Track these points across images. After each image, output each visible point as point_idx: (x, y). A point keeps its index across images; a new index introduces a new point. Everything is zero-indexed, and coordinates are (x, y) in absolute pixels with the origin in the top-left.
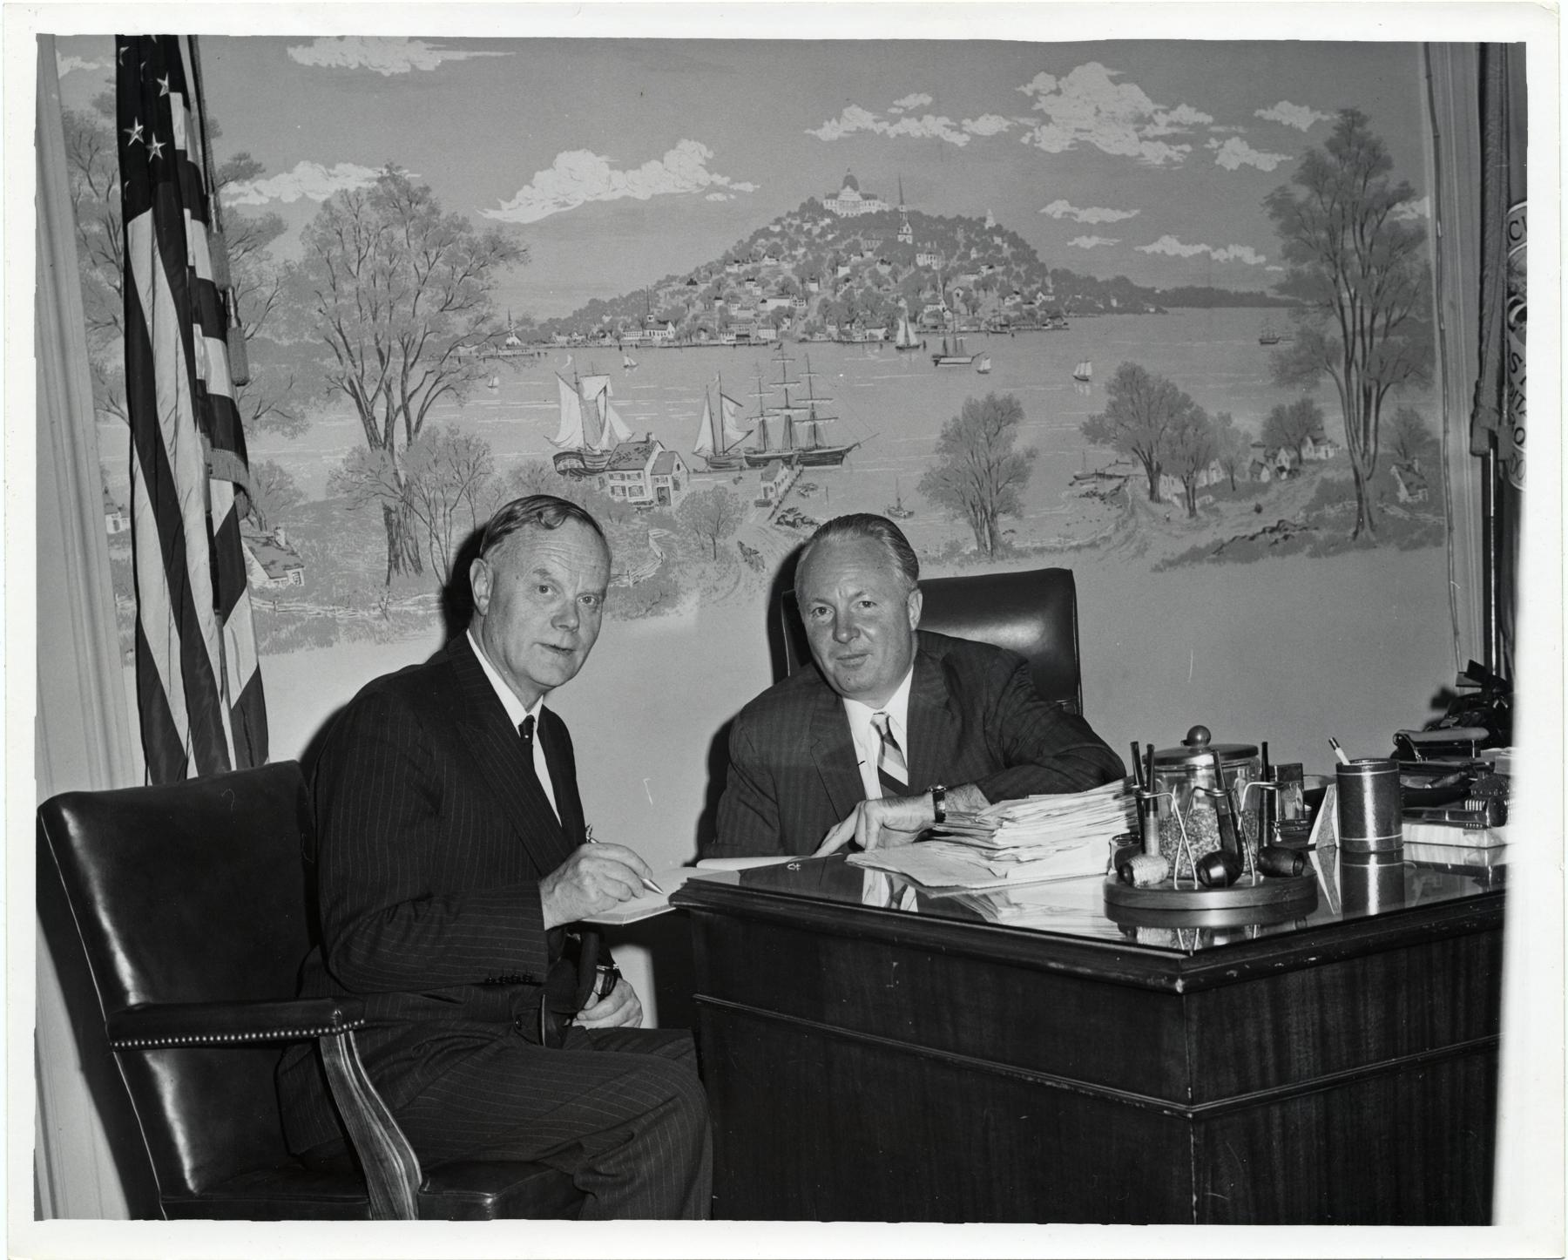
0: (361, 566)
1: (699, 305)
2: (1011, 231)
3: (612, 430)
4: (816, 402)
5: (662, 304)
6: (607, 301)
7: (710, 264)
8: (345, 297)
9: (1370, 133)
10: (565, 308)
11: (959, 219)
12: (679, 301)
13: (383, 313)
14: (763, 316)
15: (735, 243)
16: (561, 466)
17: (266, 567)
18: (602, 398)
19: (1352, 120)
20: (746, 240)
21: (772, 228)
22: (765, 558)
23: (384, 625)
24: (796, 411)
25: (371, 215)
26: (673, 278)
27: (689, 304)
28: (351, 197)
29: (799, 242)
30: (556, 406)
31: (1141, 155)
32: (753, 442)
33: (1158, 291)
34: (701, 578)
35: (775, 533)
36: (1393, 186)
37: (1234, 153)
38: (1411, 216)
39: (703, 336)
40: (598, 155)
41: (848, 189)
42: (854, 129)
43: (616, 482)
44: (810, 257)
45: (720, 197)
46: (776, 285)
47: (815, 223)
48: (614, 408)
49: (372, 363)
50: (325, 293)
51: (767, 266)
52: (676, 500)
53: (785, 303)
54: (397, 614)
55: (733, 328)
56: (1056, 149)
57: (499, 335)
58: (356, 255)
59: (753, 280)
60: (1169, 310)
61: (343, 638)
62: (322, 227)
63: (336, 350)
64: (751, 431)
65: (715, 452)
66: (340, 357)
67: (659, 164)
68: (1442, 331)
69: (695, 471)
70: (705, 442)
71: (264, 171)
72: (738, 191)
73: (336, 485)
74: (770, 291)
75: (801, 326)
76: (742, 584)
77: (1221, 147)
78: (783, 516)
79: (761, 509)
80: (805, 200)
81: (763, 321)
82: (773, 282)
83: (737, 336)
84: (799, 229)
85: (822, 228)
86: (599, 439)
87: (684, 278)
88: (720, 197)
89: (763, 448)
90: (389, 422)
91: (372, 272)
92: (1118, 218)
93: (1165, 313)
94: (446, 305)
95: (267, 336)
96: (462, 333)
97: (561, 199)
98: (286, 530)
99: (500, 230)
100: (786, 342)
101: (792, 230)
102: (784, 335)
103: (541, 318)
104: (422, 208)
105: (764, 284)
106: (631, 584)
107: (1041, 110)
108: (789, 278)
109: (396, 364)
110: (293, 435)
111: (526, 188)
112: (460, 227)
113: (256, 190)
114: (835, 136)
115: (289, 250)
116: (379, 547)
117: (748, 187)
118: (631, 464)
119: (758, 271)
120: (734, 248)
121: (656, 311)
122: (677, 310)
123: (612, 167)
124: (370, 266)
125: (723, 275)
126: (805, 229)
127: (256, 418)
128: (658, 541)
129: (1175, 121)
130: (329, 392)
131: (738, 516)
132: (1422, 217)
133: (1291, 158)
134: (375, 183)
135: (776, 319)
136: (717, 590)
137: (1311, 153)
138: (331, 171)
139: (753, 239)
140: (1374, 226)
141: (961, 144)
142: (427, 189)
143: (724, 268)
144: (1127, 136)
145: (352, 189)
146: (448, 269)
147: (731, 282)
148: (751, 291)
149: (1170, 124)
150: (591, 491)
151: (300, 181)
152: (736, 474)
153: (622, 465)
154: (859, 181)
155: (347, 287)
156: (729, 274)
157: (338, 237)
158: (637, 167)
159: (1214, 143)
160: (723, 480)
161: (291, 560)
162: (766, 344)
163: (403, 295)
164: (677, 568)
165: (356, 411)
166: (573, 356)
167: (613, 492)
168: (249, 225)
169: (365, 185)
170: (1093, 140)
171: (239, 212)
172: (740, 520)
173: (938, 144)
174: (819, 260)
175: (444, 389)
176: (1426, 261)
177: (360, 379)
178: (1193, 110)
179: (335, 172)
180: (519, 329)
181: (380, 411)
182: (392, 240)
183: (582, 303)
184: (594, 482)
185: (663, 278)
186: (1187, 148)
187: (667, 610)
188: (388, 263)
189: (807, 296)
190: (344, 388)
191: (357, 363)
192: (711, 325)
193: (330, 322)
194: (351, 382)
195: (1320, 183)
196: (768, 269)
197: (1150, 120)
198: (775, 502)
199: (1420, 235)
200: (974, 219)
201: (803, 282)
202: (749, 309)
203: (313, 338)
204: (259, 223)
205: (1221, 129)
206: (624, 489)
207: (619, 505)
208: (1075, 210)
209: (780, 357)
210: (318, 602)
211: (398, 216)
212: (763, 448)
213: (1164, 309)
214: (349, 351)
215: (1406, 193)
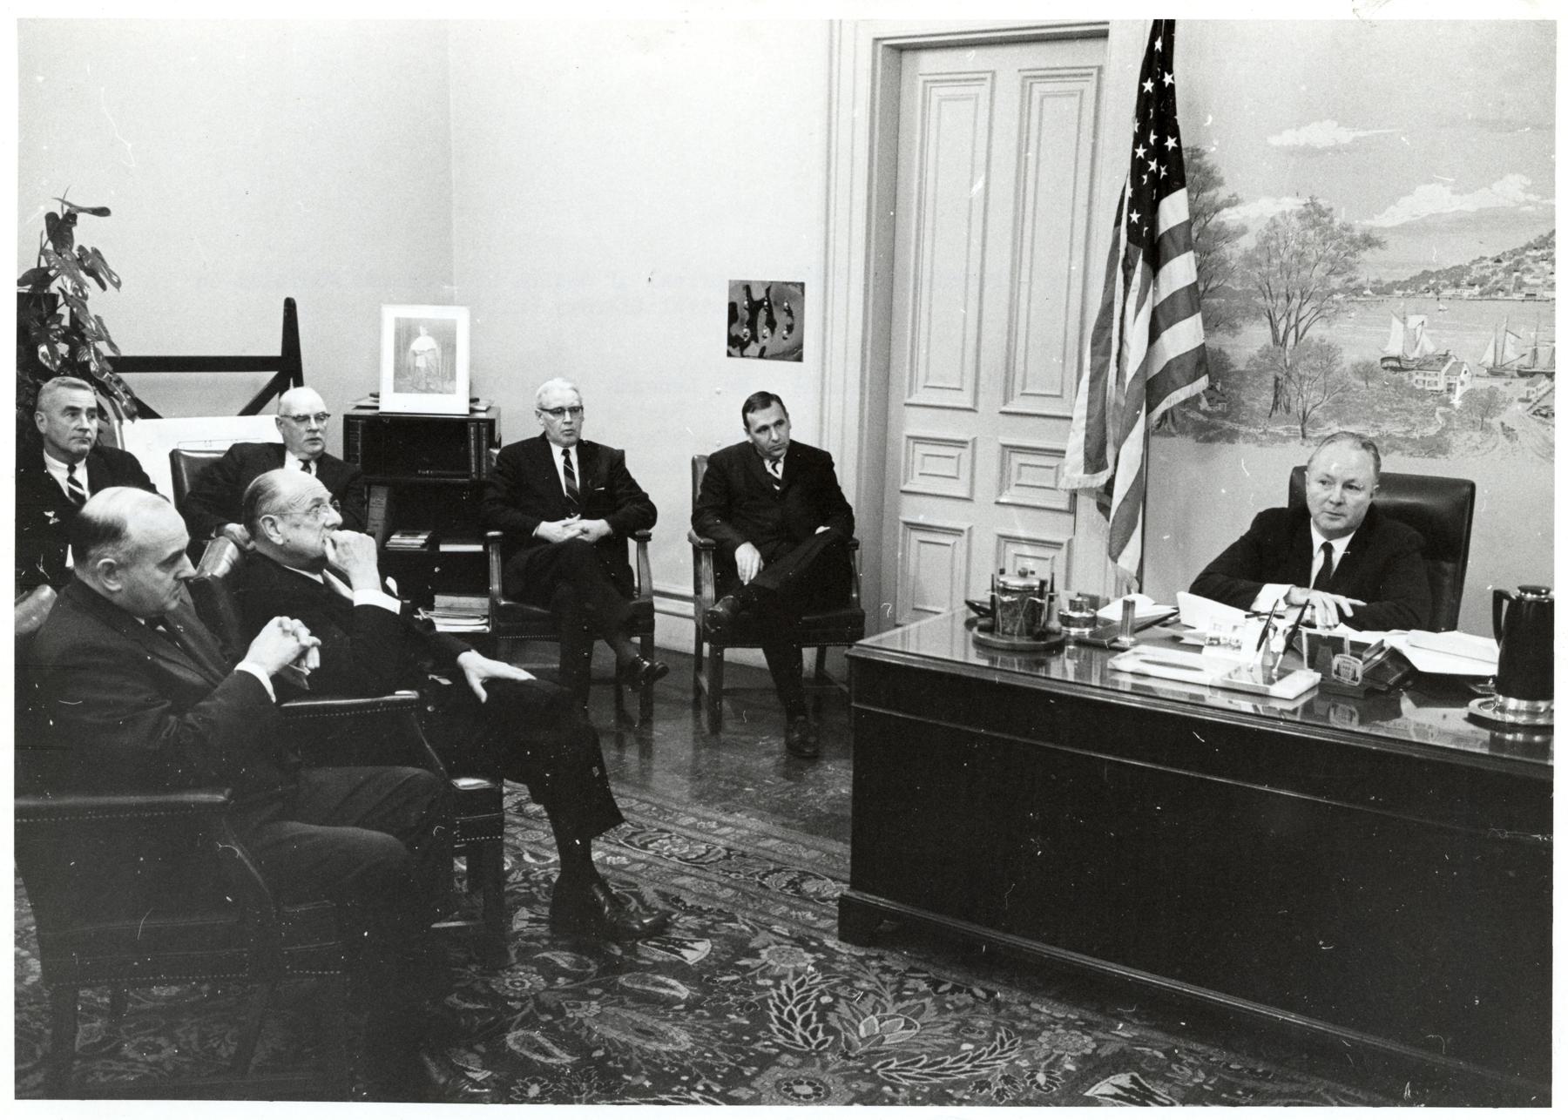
0: (1257, 406)
1: (1501, 275)
3: (1422, 347)
5: (1473, 274)
6: (1434, 270)
7: (1515, 250)
10: (1404, 275)
12: (1487, 272)
13: (1294, 275)
15: (1536, 237)
16: (1385, 364)
17: (1208, 400)
18: (1419, 328)
22: (1520, 435)
23: (1264, 437)
26: (1485, 258)
27: (1494, 273)
32: (1526, 361)
34: (1468, 439)
35: (1531, 421)
39: (1501, 294)
43: (1420, 377)
45: (1530, 208)
48: (1427, 335)
49: (1282, 301)
52: (1459, 391)
54: (1272, 433)
55: (1526, 290)
57: (1358, 290)
58: (1283, 246)
61: (1241, 441)
64: (1524, 355)
65: (1494, 364)
69: (1477, 376)
70: (1488, 358)
73: (1251, 363)
76: (1498, 448)
78: (1539, 410)
79: (1521, 404)
81: (1549, 286)
83: (1527, 295)
86: (1413, 351)
87: (1492, 259)
88: (1530, 208)
90: (1286, 333)
94: (1331, 272)
95: (1230, 285)
96: (1336, 287)
97: (1415, 213)
98: (1222, 383)
99: (1371, 231)
103: (1388, 280)
104: (1326, 220)
106: (1418, 437)
109: (1295, 302)
110: (1234, 336)
111: (1392, 207)
112: (1347, 230)
115: (1247, 243)
116: (1268, 397)
118: (1431, 368)
121: (1468, 278)
122: (1485, 276)
123: (1454, 192)
124: (1290, 250)
125: (1523, 257)
127: (1217, 326)
128: (1441, 414)
131: (1503, 405)
134: (1301, 207)
136: (1478, 448)
142: (1331, 210)
143: (1524, 253)
145: (1288, 210)
146: (1334, 253)
147: (1529, 261)
148: (1543, 268)
150: (1402, 381)
152: (1508, 380)
153: (1426, 367)
155: (1275, 261)
156: (1528, 256)
160: (1498, 383)
161: (1222, 398)
163: (1307, 265)
164: (1451, 433)
165: (1269, 326)
167: (1417, 381)
169: (1297, 208)
172: (1504, 409)
175: (1321, 317)
177: (1274, 309)
180: (1373, 286)
181: (1282, 327)
182: (1306, 236)
183: (1417, 271)
184: (1405, 375)
185: (1477, 258)
187: (1439, 456)
188: (1300, 249)
192: (1507, 287)
194: (1269, 312)
198: (1535, 401)
202: (1538, 278)
206: (1424, 382)
207: (1419, 390)
210: (1232, 421)
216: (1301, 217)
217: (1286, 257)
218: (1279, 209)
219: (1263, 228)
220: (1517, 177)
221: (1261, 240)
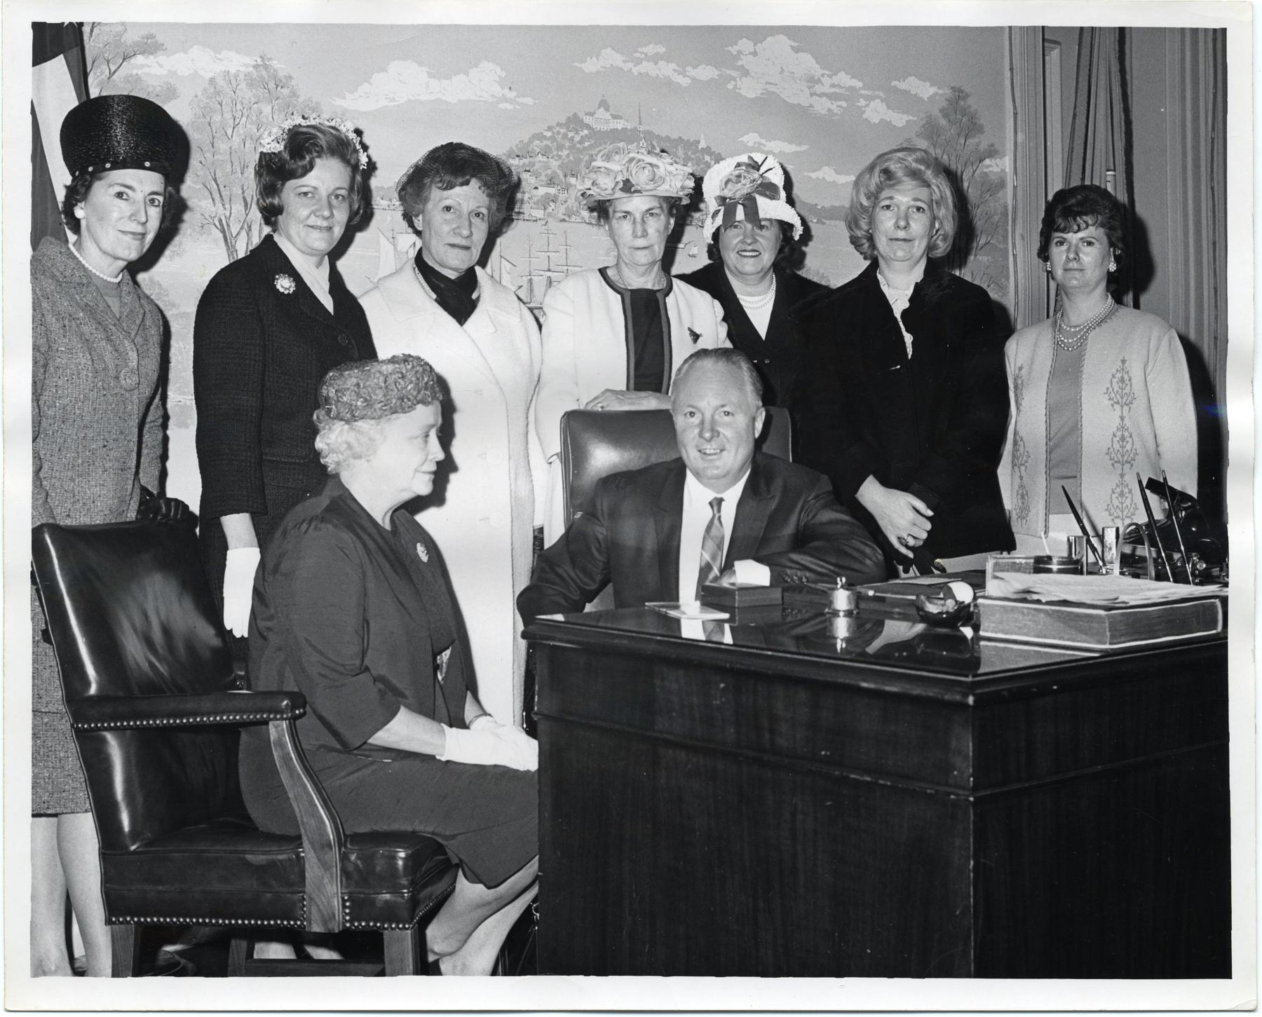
2: (717, 152)
4: (569, 268)
8: (221, 154)
9: (970, 106)
11: (680, 138)
14: (535, 199)
19: (959, 95)
20: (526, 141)
21: (545, 133)
24: (556, 274)
25: (246, 93)
28: (232, 78)
29: (564, 145)
30: (378, 254)
31: (811, 106)
33: (819, 207)
36: (984, 146)
37: (876, 111)
38: (996, 169)
40: (420, 64)
41: (602, 109)
42: (608, 66)
44: (571, 158)
45: (509, 107)
46: (547, 175)
47: (577, 133)
50: (204, 149)
51: (540, 161)
53: (552, 191)
56: (751, 95)
59: (529, 171)
60: (827, 222)
62: (207, 98)
63: (211, 194)
66: (213, 200)
67: (465, 77)
68: (1014, 256)
71: (166, 49)
72: (522, 103)
74: (542, 181)
75: (562, 209)
77: (867, 105)
80: (571, 115)
81: (534, 203)
82: (543, 174)
84: (565, 136)
85: (582, 137)
88: (509, 107)
89: (529, 301)
91: (243, 137)
92: (793, 150)
93: (823, 223)
97: (391, 96)
100: (550, 220)
101: (560, 136)
102: (550, 215)
104: (285, 91)
105: (537, 175)
107: (742, 66)
108: (556, 173)
113: (158, 62)
114: (594, 70)
117: (529, 101)
119: (533, 164)
120: (516, 146)
123: (430, 75)
124: (241, 132)
126: (569, 136)
129: (836, 83)
130: (202, 227)
132: (1003, 171)
133: (915, 119)
134: (251, 69)
135: (546, 201)
137: (930, 117)
138: (219, 56)
139: (531, 141)
140: (970, 174)
141: (684, 85)
144: (802, 91)
145: (233, 71)
149: (833, 86)
151: (193, 60)
154: (610, 103)
155: (222, 146)
157: (219, 106)
158: (448, 77)
159: (862, 102)
162: (536, 221)
166: (392, 216)
168: (151, 89)
169: (243, 69)
170: (778, 92)
171: (144, 78)
173: (668, 82)
174: (581, 160)
176: (1005, 203)
177: (228, 219)
178: (849, 76)
179: (219, 56)
182: (261, 113)
186: (844, 104)
189: (567, 188)
190: (215, 224)
191: (226, 206)
193: (208, 173)
194: (220, 221)
195: (935, 139)
196: (540, 164)
197: (819, 81)
199: (1002, 184)
200: (691, 141)
201: (565, 176)
203: (195, 183)
204: (158, 89)
205: (869, 93)
208: (763, 141)
209: (546, 232)
211: (267, 95)
212: (529, 301)
213: (824, 221)
214: (221, 196)
215: (992, 153)
216: (251, 83)
217: (236, 140)
218: (219, 68)
219: (199, 94)
220: (491, 65)
221: (199, 112)
